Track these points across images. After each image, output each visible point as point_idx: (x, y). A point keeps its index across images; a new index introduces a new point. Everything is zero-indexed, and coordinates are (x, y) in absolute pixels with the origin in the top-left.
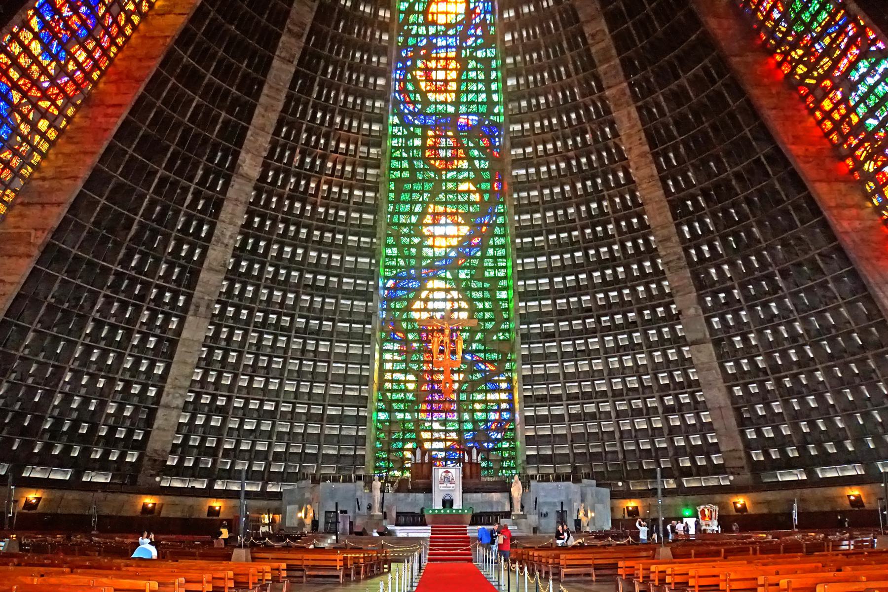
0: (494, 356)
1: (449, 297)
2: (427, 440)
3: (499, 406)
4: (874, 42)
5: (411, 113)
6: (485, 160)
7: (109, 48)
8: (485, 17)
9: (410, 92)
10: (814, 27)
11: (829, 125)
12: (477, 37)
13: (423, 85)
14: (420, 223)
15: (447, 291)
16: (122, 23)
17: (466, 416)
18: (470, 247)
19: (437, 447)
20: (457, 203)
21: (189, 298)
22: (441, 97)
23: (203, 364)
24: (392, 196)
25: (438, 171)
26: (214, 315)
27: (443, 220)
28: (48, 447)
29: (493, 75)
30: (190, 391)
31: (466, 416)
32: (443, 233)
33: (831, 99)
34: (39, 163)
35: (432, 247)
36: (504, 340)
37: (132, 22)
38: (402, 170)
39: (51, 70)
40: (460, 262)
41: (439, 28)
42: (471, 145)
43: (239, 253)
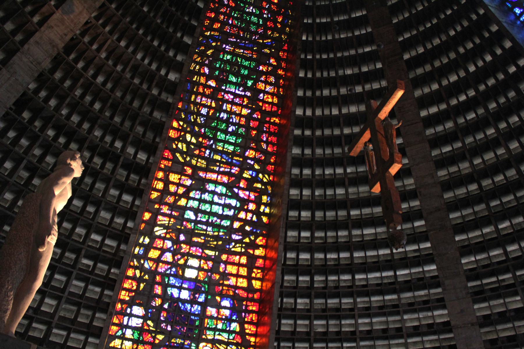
10: (218, 144)
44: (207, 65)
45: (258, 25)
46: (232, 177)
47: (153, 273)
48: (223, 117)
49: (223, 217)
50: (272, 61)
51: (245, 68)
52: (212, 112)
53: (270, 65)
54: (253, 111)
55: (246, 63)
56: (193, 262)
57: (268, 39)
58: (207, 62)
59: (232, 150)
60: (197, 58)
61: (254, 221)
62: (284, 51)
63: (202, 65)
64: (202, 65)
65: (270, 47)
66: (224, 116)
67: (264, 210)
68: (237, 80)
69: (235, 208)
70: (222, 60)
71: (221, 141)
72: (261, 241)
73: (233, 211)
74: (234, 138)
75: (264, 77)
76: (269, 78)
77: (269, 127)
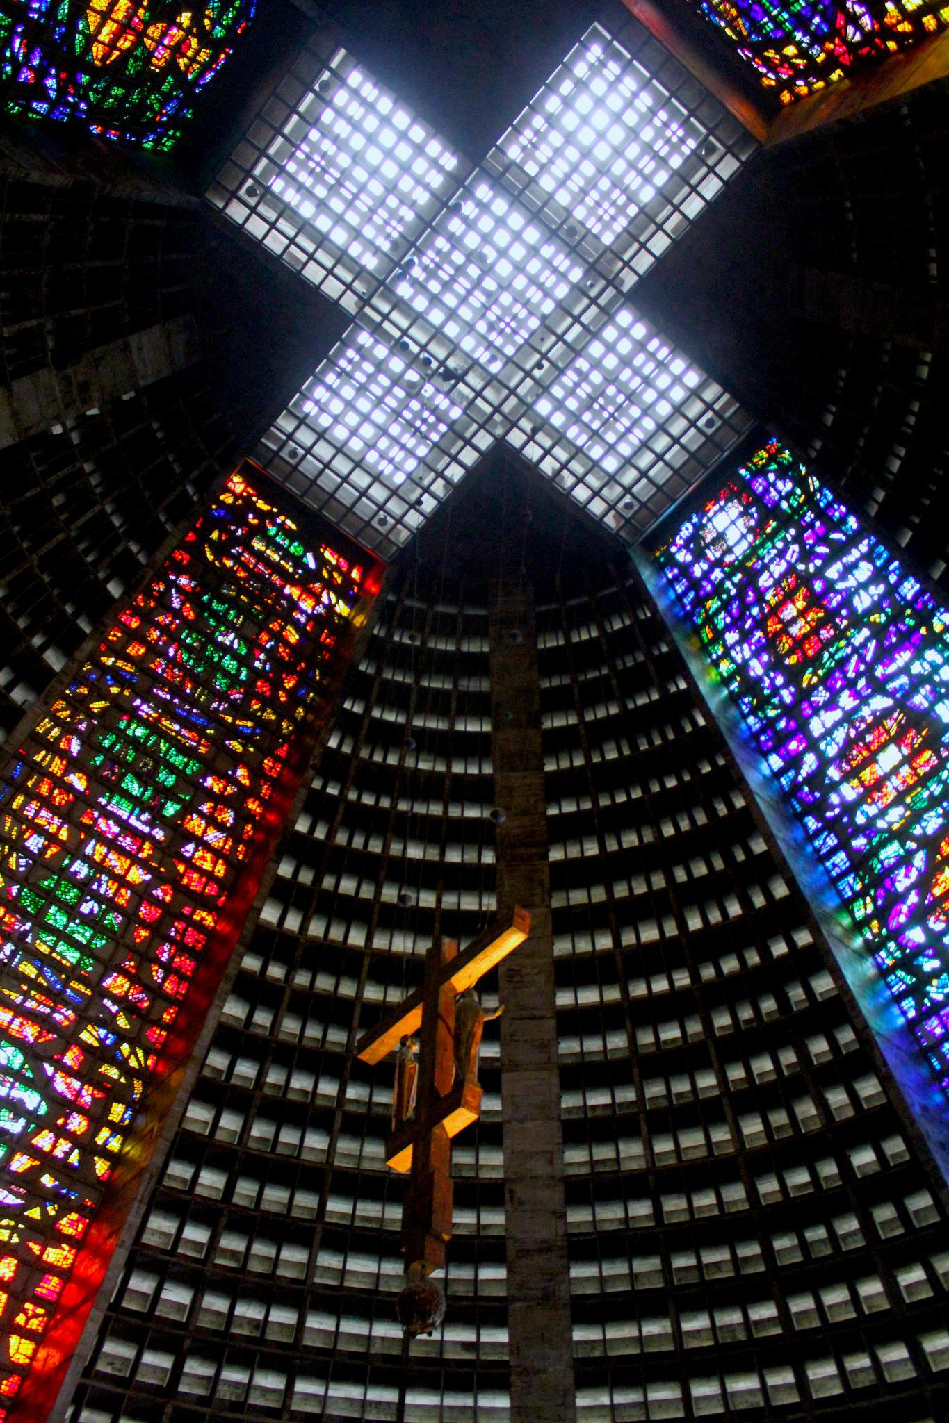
44: (79, 734)
45: (234, 679)
46: (49, 1032)
48: (76, 873)
50: (241, 772)
51: (172, 769)
52: (53, 850)
53: (234, 781)
54: (159, 879)
55: (178, 760)
57: (247, 718)
58: (83, 727)
59: (74, 961)
60: (63, 709)
61: (72, 1165)
62: (277, 759)
63: (69, 729)
64: (69, 729)
65: (246, 739)
66: (81, 869)
67: (106, 1142)
68: (143, 794)
69: (31, 1116)
70: (121, 734)
71: (51, 930)
72: (72, 1224)
73: (22, 1122)
74: (88, 934)
75: (209, 805)
76: (221, 810)
77: (185, 930)
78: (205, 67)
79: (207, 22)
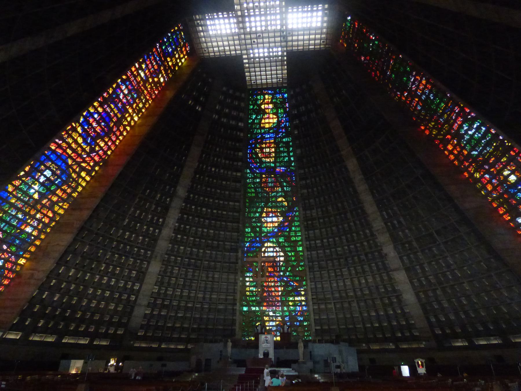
0: (298, 278)
1: (275, 250)
2: (267, 321)
3: (301, 303)
4: (469, 114)
5: (255, 167)
6: (289, 187)
7: (115, 141)
8: (286, 124)
9: (255, 158)
11: (452, 157)
12: (283, 133)
13: (260, 155)
14: (261, 217)
15: (274, 247)
16: (122, 130)
17: (285, 309)
18: (284, 226)
19: (272, 325)
20: (277, 207)
21: (153, 252)
22: (268, 160)
23: (158, 284)
24: (248, 204)
25: (268, 193)
26: (164, 260)
27: (271, 215)
28: (78, 326)
29: (291, 149)
30: (151, 297)
31: (285, 309)
32: (271, 221)
33: (452, 144)
34: (81, 191)
35: (267, 227)
36: (301, 270)
37: (126, 130)
38: (251, 193)
39: (88, 149)
40: (279, 234)
41: (266, 130)
42: (282, 180)
43: (177, 231)
47: (501, 196)
49: (484, 136)
56: (506, 173)
66: (424, 97)
78: (269, 94)
79: (261, 101)
